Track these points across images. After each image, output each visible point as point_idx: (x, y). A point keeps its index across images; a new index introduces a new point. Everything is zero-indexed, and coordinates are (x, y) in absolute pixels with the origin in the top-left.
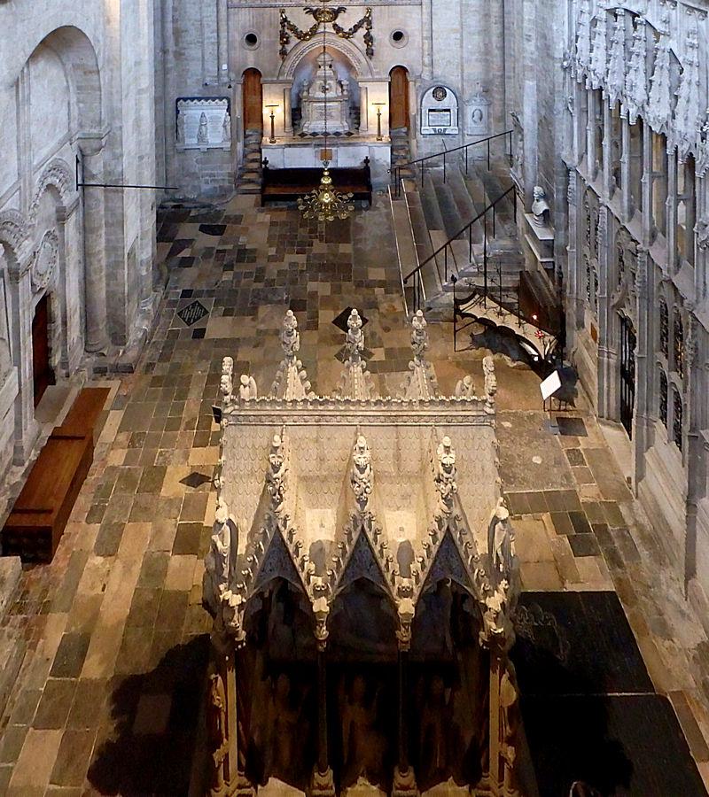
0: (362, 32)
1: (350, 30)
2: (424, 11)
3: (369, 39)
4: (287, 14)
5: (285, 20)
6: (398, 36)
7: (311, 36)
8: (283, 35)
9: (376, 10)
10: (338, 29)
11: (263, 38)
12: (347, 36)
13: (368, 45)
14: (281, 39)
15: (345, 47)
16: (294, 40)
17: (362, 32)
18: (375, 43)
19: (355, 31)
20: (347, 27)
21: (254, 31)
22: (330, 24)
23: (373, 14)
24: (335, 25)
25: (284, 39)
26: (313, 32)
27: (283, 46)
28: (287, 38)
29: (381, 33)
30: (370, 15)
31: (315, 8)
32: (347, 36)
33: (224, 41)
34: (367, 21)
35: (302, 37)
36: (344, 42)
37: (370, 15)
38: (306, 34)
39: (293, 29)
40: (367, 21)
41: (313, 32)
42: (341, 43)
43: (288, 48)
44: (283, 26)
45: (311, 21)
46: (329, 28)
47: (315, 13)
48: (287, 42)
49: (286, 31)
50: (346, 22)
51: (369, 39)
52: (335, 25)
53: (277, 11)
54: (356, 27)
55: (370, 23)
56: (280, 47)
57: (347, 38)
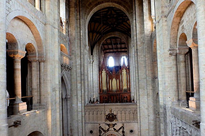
0: (121, 130)
1: (118, 129)
2: (138, 124)
3: (123, 132)
4: (101, 125)
5: (100, 127)
6: (131, 131)
7: (107, 131)
8: (100, 131)
9: (125, 124)
10: (115, 129)
11: (95, 132)
12: (117, 131)
13: (123, 134)
14: (99, 132)
15: (117, 134)
16: (103, 132)
17: (121, 130)
18: (125, 133)
19: (119, 130)
20: (117, 129)
21: (92, 130)
22: (113, 128)
23: (124, 125)
24: (114, 128)
25: (100, 132)
26: (108, 130)
27: (100, 134)
28: (101, 132)
29: (127, 130)
30: (123, 126)
31: (108, 124)
32: (117, 131)
33: (84, 132)
34: (123, 127)
35: (105, 131)
36: (116, 133)
37: (123, 126)
38: (106, 131)
39: (103, 129)
40: (123, 127)
41: (108, 130)
42: (116, 133)
43: (101, 134)
44: (100, 129)
45: (107, 127)
46: (112, 129)
47: (109, 125)
48: (101, 133)
49: (101, 130)
50: (117, 127)
51: (123, 132)
52: (114, 128)
53: (98, 124)
54: (120, 129)
55: (123, 128)
56: (99, 134)
57: (117, 132)
